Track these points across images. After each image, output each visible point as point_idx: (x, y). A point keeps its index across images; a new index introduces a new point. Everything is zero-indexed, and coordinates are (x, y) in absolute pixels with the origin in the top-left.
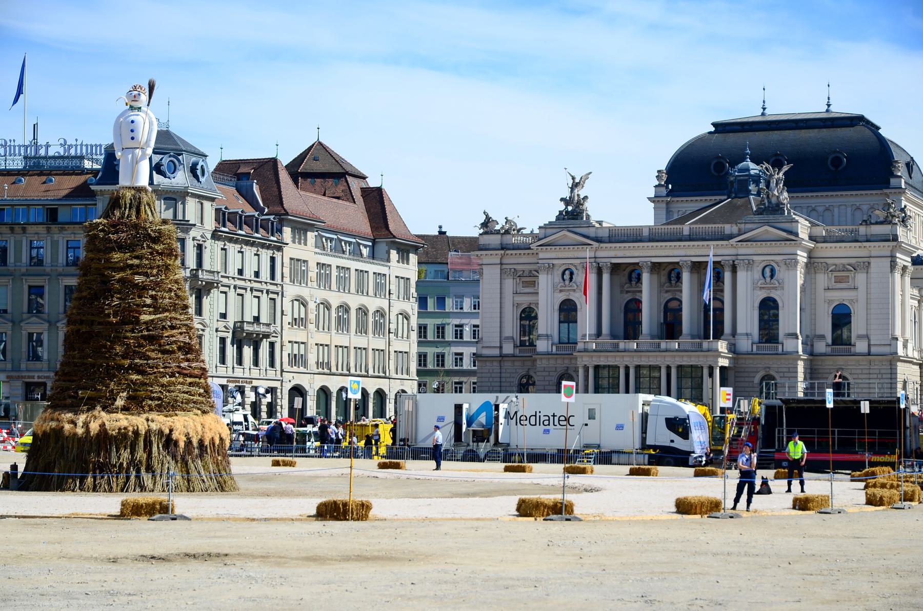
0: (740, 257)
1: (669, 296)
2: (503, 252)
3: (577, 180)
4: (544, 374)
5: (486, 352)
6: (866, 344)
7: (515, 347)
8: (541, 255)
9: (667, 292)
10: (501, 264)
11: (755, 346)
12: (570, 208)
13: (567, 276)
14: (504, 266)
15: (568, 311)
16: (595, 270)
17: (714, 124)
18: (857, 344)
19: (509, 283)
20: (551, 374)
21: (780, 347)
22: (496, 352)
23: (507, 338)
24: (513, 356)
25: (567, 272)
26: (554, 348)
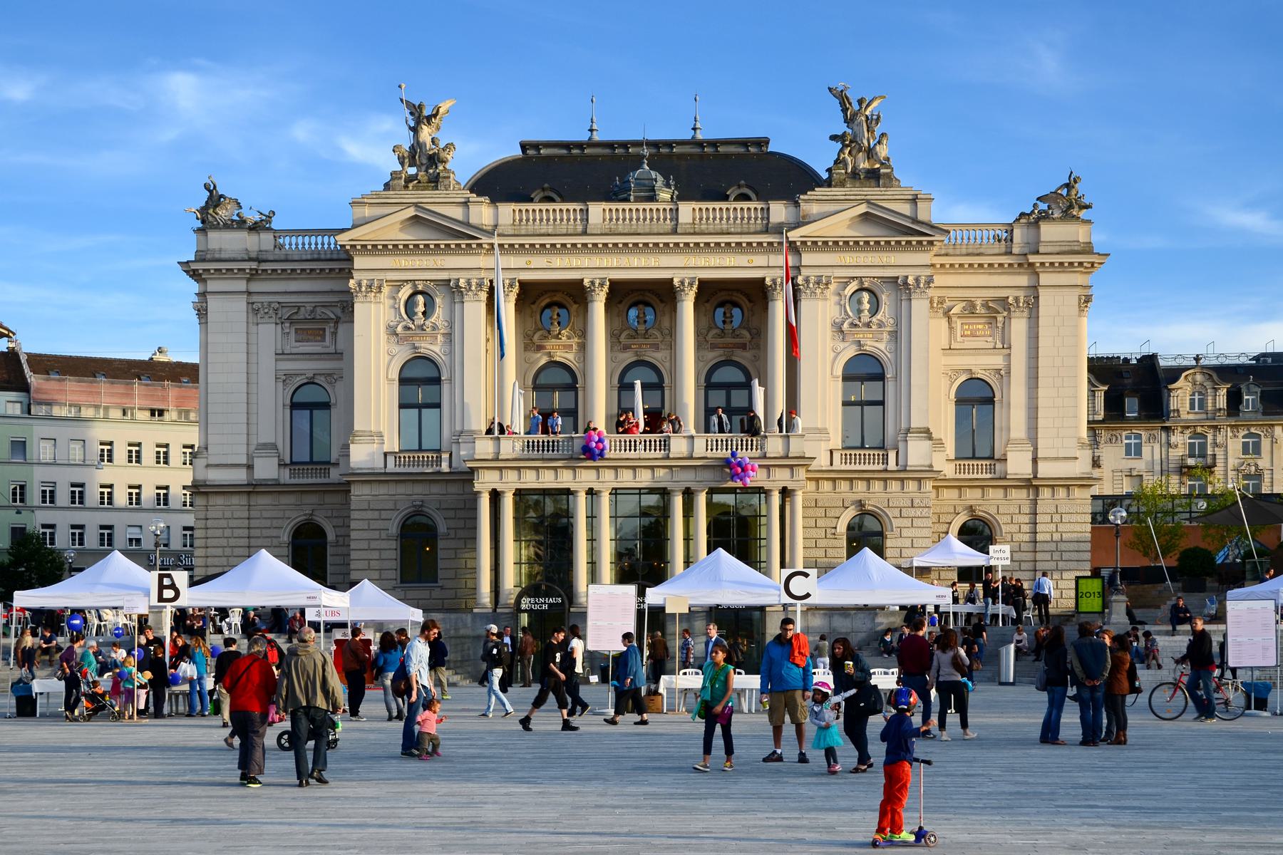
0: (804, 272)
1: (629, 357)
2: (254, 265)
3: (426, 112)
4: (370, 515)
5: (216, 476)
6: (1030, 456)
7: (282, 465)
8: (359, 262)
9: (626, 348)
10: (249, 293)
11: (837, 456)
12: (412, 171)
13: (421, 308)
14: (255, 298)
15: (422, 384)
16: (483, 296)
17: (524, 146)
18: (1010, 456)
19: (269, 334)
20: (384, 515)
21: (892, 455)
22: (240, 476)
23: (264, 446)
24: (277, 483)
25: (420, 299)
26: (391, 459)
